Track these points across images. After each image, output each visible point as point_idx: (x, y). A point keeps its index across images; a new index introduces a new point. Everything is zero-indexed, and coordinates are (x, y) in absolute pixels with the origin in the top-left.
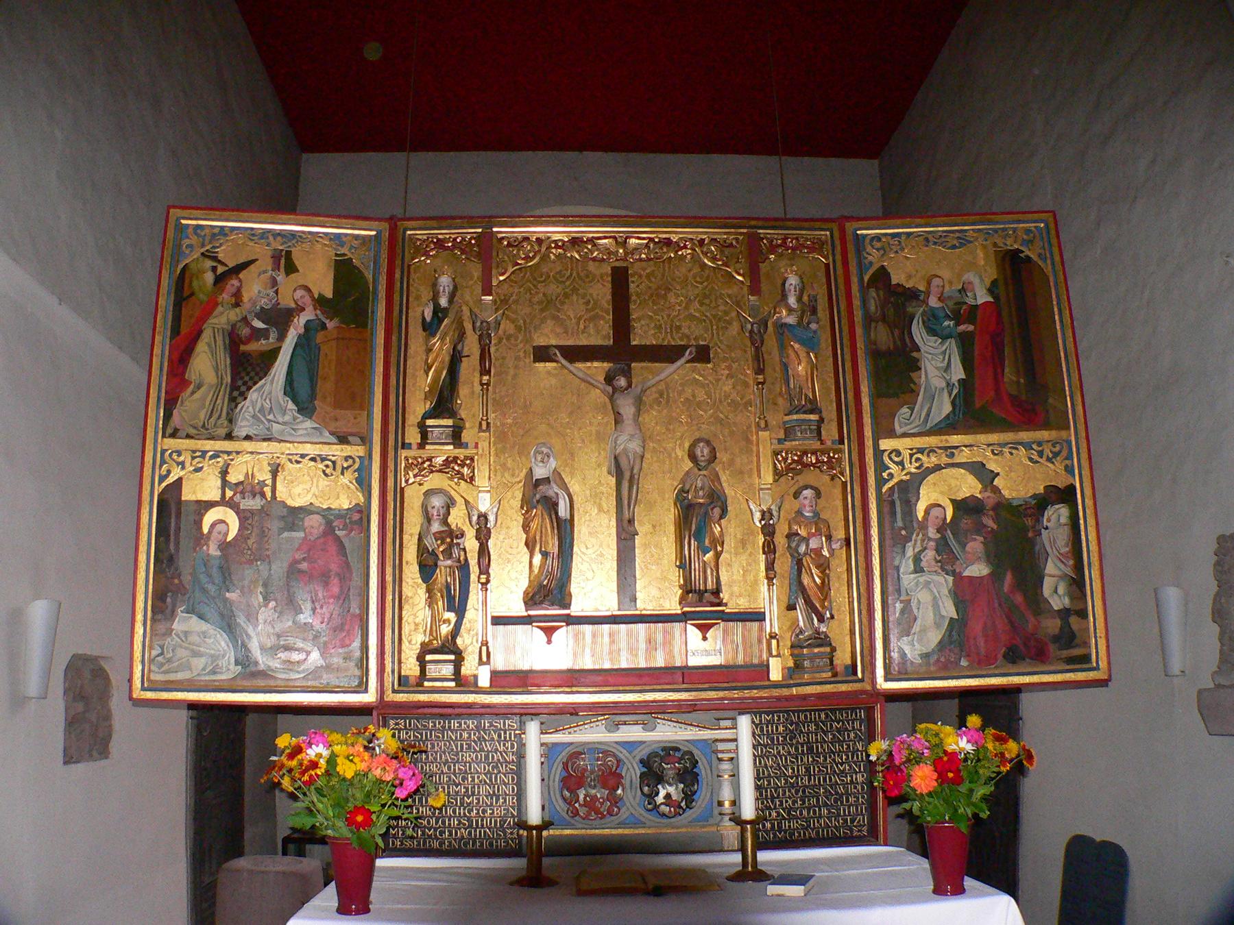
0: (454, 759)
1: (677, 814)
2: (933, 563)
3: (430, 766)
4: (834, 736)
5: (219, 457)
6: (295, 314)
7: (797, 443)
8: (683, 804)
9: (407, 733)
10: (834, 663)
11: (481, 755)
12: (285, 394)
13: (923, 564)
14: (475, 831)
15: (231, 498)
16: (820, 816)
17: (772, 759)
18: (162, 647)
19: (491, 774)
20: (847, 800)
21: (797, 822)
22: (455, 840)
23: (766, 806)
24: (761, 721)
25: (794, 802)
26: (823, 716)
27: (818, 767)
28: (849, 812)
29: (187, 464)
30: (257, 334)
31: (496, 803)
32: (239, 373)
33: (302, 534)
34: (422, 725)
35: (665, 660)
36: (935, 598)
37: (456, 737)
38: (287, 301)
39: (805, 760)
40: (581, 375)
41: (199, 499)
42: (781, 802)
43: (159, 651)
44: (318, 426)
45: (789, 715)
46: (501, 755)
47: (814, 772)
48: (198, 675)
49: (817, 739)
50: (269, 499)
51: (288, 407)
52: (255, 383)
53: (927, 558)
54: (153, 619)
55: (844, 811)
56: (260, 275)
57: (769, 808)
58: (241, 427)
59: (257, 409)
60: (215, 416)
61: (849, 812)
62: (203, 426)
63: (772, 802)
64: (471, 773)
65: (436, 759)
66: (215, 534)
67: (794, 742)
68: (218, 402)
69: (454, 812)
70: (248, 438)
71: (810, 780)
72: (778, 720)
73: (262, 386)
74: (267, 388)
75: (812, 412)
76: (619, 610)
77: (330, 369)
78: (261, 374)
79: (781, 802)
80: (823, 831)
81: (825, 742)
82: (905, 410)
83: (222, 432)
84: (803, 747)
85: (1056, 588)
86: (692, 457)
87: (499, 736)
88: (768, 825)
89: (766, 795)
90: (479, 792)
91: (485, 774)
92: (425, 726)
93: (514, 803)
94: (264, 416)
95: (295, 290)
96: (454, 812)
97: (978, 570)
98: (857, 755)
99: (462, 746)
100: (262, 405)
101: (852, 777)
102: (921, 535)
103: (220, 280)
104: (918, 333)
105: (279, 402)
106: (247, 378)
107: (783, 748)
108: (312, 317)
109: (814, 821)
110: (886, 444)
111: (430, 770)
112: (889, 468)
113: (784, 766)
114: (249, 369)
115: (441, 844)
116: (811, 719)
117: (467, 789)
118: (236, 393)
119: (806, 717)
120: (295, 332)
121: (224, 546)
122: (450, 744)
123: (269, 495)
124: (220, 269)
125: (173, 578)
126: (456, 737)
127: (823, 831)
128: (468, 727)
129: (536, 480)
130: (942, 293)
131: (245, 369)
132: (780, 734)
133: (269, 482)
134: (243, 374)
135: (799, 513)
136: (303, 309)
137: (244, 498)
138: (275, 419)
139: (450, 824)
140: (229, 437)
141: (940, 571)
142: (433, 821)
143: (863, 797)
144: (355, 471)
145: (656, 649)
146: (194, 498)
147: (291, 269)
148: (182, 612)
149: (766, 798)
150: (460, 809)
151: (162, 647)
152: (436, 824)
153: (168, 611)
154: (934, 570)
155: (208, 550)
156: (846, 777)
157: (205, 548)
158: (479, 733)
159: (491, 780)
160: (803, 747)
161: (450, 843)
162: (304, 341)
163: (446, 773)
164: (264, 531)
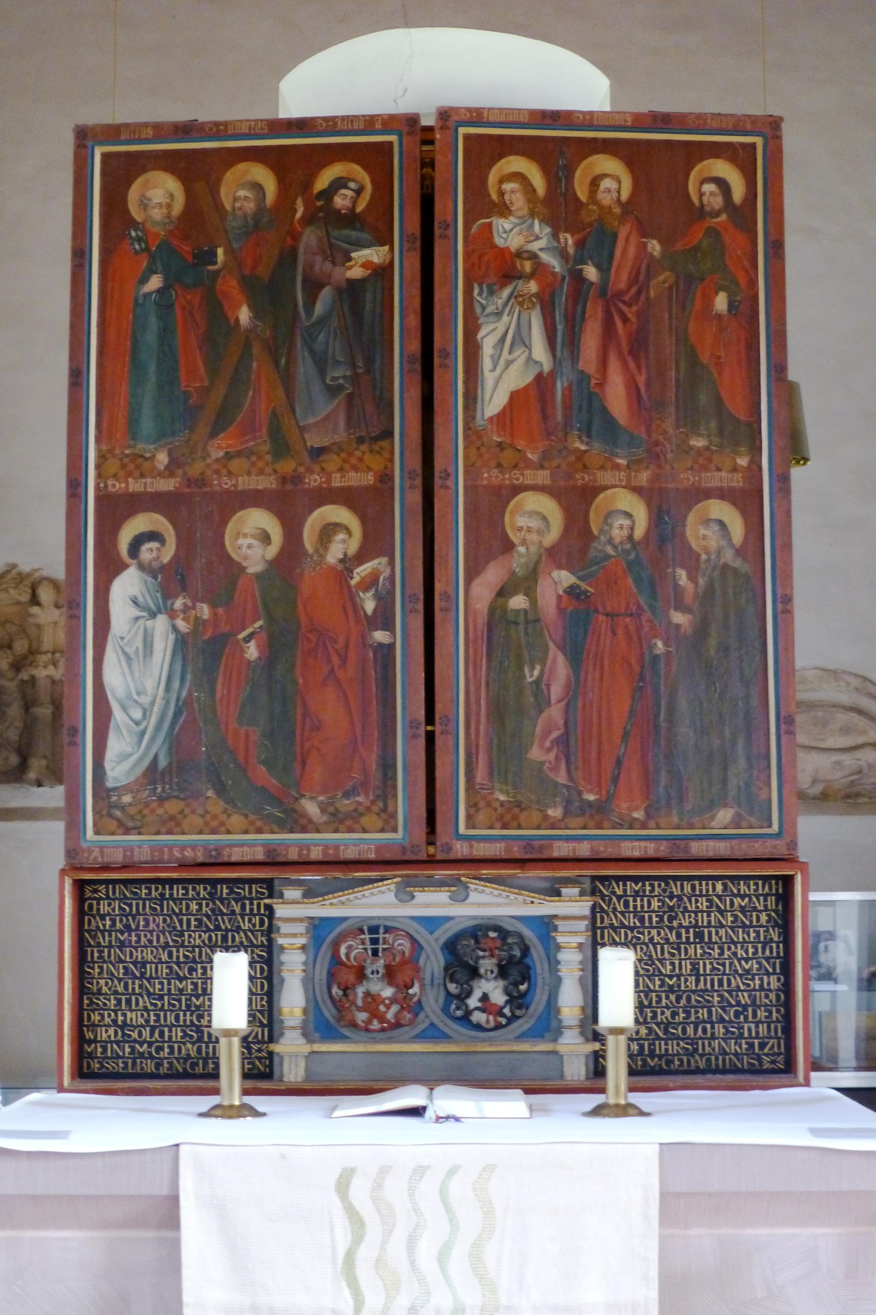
0: (176, 941)
1: (498, 1027)
3: (142, 952)
4: (736, 917)
8: (507, 1011)
9: (109, 905)
11: (216, 935)
14: (207, 1047)
16: (713, 1037)
17: (642, 949)
20: (755, 1015)
21: (678, 1045)
22: (177, 1059)
24: (625, 891)
25: (674, 1014)
26: (719, 887)
27: (711, 963)
28: (757, 1033)
34: (132, 893)
37: (181, 910)
39: (691, 951)
42: (655, 1014)
45: (667, 884)
46: (247, 936)
47: (705, 970)
49: (709, 922)
55: (750, 1030)
61: (757, 1033)
64: (202, 962)
65: (150, 941)
67: (675, 923)
69: (177, 1018)
71: (698, 981)
72: (652, 891)
79: (655, 1014)
80: (717, 1059)
81: (722, 926)
84: (687, 932)
87: (243, 907)
92: (136, 894)
93: (263, 1006)
96: (177, 1018)
98: (771, 949)
99: (189, 921)
101: (761, 980)
107: (659, 934)
109: (703, 1044)
111: (143, 958)
113: (659, 960)
115: (158, 1066)
116: (701, 890)
117: (195, 985)
119: (693, 888)
122: (171, 918)
126: (181, 910)
127: (717, 1059)
128: (198, 894)
132: (653, 911)
139: (170, 1037)
142: (146, 1033)
143: (778, 1011)
150: (185, 1015)
152: (151, 1036)
156: (753, 979)
158: (214, 904)
160: (687, 932)
161: (171, 1064)
163: (167, 962)
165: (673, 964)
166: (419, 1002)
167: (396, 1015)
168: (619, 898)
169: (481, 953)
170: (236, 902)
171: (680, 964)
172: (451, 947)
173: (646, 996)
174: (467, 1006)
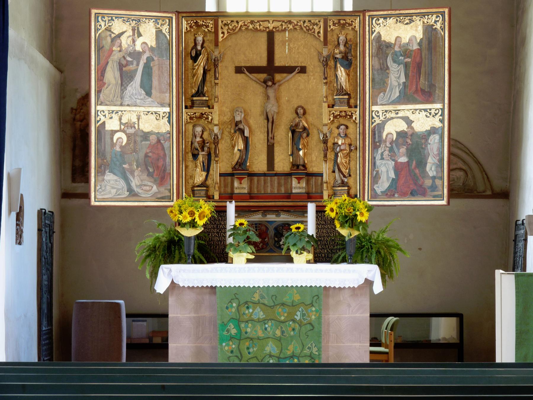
2: (388, 156)
5: (118, 113)
7: (338, 107)
10: (350, 193)
12: (141, 87)
13: (384, 156)
15: (123, 129)
18: (101, 186)
19: (219, 233)
23: (323, 248)
24: (321, 215)
29: (107, 116)
30: (128, 63)
31: (221, 244)
35: (285, 190)
36: (388, 169)
38: (138, 48)
40: (254, 79)
42: (329, 247)
43: (100, 187)
44: (152, 100)
46: (223, 226)
52: (130, 83)
53: (386, 154)
54: (97, 175)
57: (324, 249)
59: (131, 94)
60: (116, 96)
63: (325, 246)
64: (211, 233)
66: (118, 143)
68: (116, 91)
70: (128, 105)
74: (134, 84)
75: (345, 95)
76: (268, 171)
79: (329, 247)
82: (382, 94)
83: (119, 103)
85: (431, 168)
86: (297, 113)
88: (323, 255)
89: (323, 244)
90: (214, 240)
91: (217, 233)
94: (134, 97)
95: (142, 44)
97: (403, 159)
102: (384, 145)
103: (113, 40)
104: (389, 62)
106: (126, 81)
107: (330, 226)
108: (148, 56)
110: (375, 108)
112: (375, 118)
118: (123, 88)
120: (143, 62)
121: (121, 147)
123: (137, 127)
124: (113, 35)
125: (104, 160)
129: (236, 121)
130: (400, 45)
133: (137, 123)
135: (339, 134)
140: (121, 105)
141: (390, 159)
144: (167, 118)
145: (281, 186)
146: (110, 129)
147: (140, 35)
148: (108, 172)
149: (323, 245)
151: (101, 186)
154: (388, 159)
155: (116, 148)
157: (115, 148)
159: (219, 235)
164: (135, 142)
165: (334, 234)
166: (268, 243)
167: (262, 246)
168: (320, 217)
169: (284, 230)
170: (220, 217)
171: (335, 234)
172: (276, 229)
173: (326, 242)
174: (280, 244)
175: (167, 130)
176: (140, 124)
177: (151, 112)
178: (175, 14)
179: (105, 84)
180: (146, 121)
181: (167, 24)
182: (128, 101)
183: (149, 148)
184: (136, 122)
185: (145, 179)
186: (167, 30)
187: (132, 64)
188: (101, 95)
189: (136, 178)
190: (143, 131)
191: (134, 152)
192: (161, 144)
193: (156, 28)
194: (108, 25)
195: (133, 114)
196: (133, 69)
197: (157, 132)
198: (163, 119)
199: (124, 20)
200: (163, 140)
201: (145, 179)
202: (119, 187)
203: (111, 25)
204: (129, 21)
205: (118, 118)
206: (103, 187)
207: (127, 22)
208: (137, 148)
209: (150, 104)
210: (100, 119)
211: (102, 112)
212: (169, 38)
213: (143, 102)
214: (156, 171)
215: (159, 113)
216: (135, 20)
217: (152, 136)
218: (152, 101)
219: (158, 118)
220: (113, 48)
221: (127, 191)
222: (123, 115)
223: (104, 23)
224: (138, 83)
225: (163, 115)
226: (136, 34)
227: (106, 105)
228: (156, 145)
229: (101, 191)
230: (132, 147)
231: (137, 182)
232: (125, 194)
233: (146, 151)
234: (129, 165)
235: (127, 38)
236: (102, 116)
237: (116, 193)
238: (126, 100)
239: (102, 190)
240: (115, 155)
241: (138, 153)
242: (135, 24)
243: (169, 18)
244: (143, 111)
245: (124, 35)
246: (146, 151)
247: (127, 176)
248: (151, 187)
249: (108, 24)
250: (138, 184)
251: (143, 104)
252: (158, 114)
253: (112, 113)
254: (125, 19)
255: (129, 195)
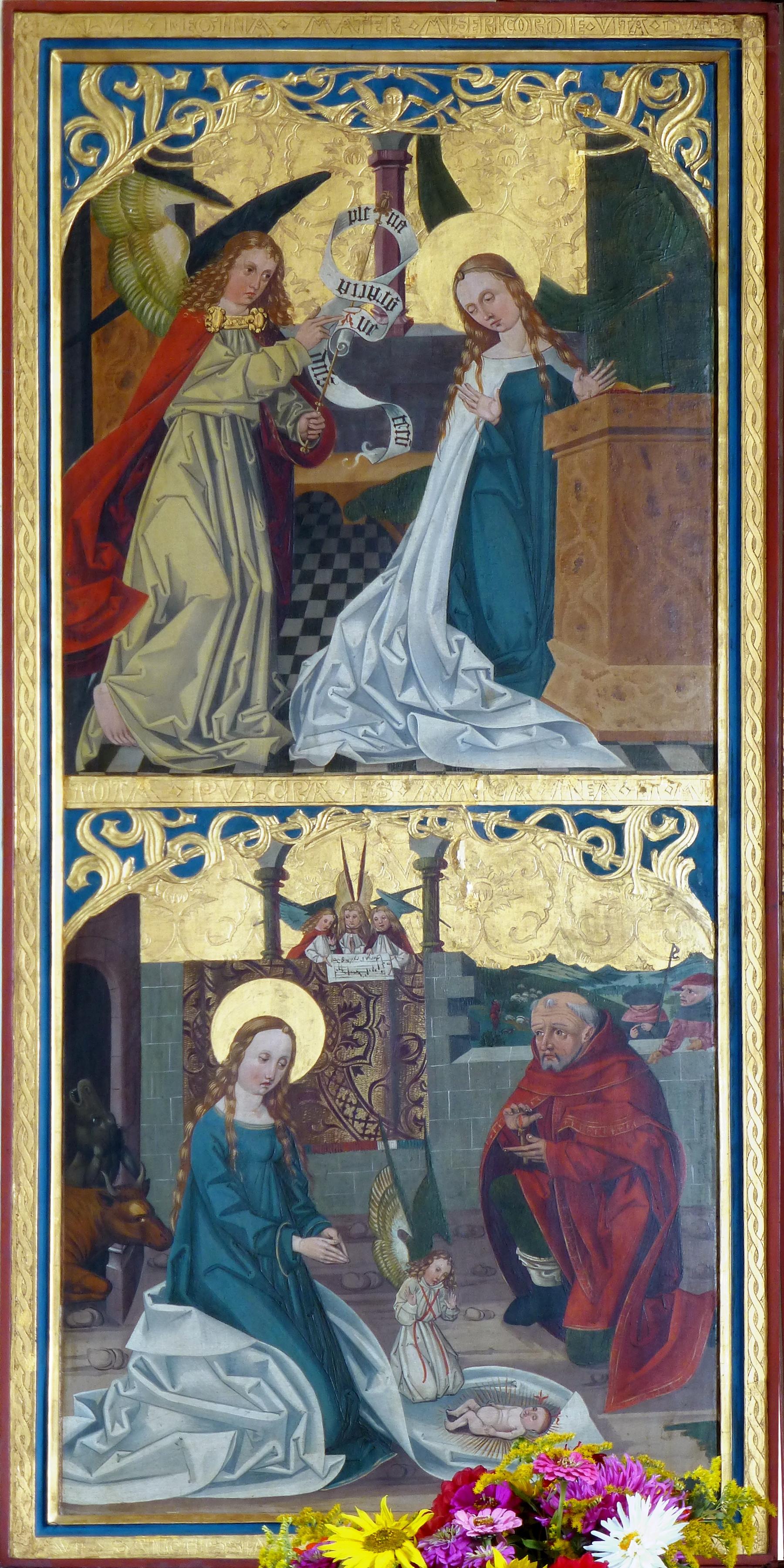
6: (465, 356)
12: (452, 620)
15: (299, 951)
18: (97, 1407)
29: (152, 855)
32: (299, 560)
33: (524, 1053)
41: (196, 958)
43: (90, 1418)
44: (557, 717)
48: (213, 1485)
50: (418, 950)
51: (466, 663)
52: (354, 591)
54: (67, 1326)
56: (338, 227)
58: (316, 732)
59: (366, 674)
62: (196, 734)
66: (250, 1060)
68: (237, 655)
73: (380, 596)
77: (591, 534)
78: (372, 560)
95: (461, 273)
100: (381, 660)
105: (434, 647)
106: (324, 577)
108: (526, 364)
114: (331, 546)
118: (292, 627)
120: (471, 417)
123: (415, 932)
131: (315, 547)
133: (415, 899)
134: (311, 562)
136: (492, 338)
137: (339, 951)
138: (425, 706)
146: (179, 955)
148: (155, 1299)
151: (97, 1407)
153: (116, 1297)
155: (232, 1110)
157: (221, 1105)
162: (499, 443)
164: (405, 1050)
175: (683, 956)
176: (447, 910)
177: (541, 815)
178: (766, 17)
179: (134, 599)
180: (499, 882)
181: (694, 101)
182: (340, 728)
183: (520, 1094)
184: (409, 898)
185: (491, 1350)
186: (693, 155)
187: (380, 440)
188: (101, 693)
189: (405, 1337)
190: (468, 965)
191: (396, 1135)
192: (634, 1060)
193: (593, 142)
194: (164, 133)
195: (386, 829)
196: (391, 473)
197: (593, 967)
198: (646, 862)
199: (304, 88)
200: (650, 1035)
201: (491, 1350)
202: (255, 1415)
203: (189, 130)
204: (353, 96)
205: (249, 870)
206: (116, 1419)
207: (333, 99)
208: (419, 1102)
209: (532, 747)
210: (94, 879)
211: (110, 830)
212: (708, 219)
213: (470, 733)
214: (584, 1286)
215: (614, 818)
216: (406, 87)
217: (550, 998)
218: (546, 725)
219: (604, 856)
220: (201, 313)
221: (330, 1450)
222: (298, 843)
223: (129, 124)
224: (424, 589)
225: (654, 837)
226: (410, 192)
227: (148, 767)
228: (588, 1070)
229: (103, 1448)
230: (378, 1091)
231: (415, 1370)
232: (307, 1467)
233: (501, 1118)
234: (346, 1236)
235: (328, 230)
236: (112, 857)
237: (230, 1466)
238: (325, 720)
239: (106, 1438)
240: (226, 1160)
241: (425, 1143)
242: (405, 116)
243: (706, 55)
244: (475, 809)
245: (301, 208)
246: (501, 1118)
247: (328, 1325)
248: (541, 1413)
249: (162, 124)
250: (429, 1389)
251: (476, 749)
252: (605, 824)
253: (202, 827)
254: (313, 77)
255: (343, 1475)
